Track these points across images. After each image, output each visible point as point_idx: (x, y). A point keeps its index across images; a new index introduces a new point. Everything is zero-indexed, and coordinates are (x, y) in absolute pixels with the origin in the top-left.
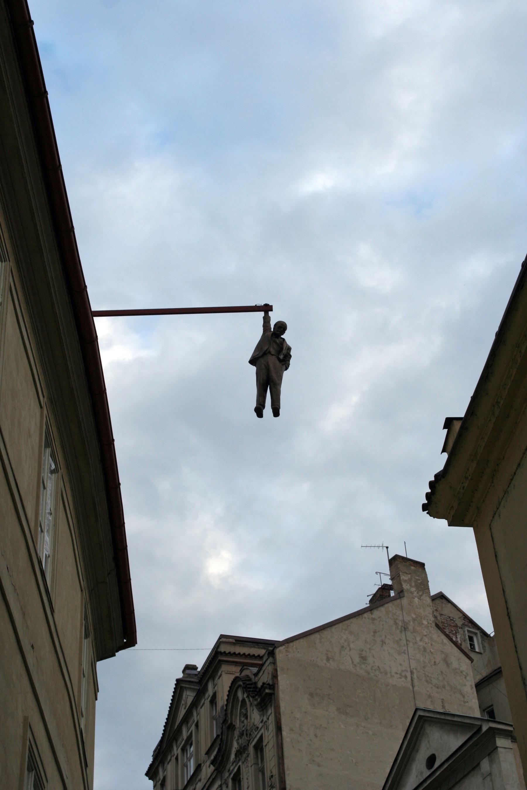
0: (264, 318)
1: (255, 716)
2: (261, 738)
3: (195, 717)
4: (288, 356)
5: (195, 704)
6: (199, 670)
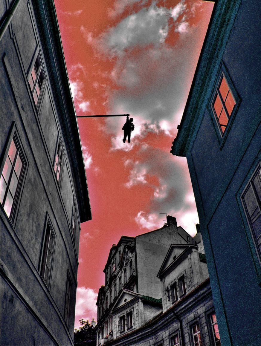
0: (127, 118)
1: (130, 255)
2: (131, 260)
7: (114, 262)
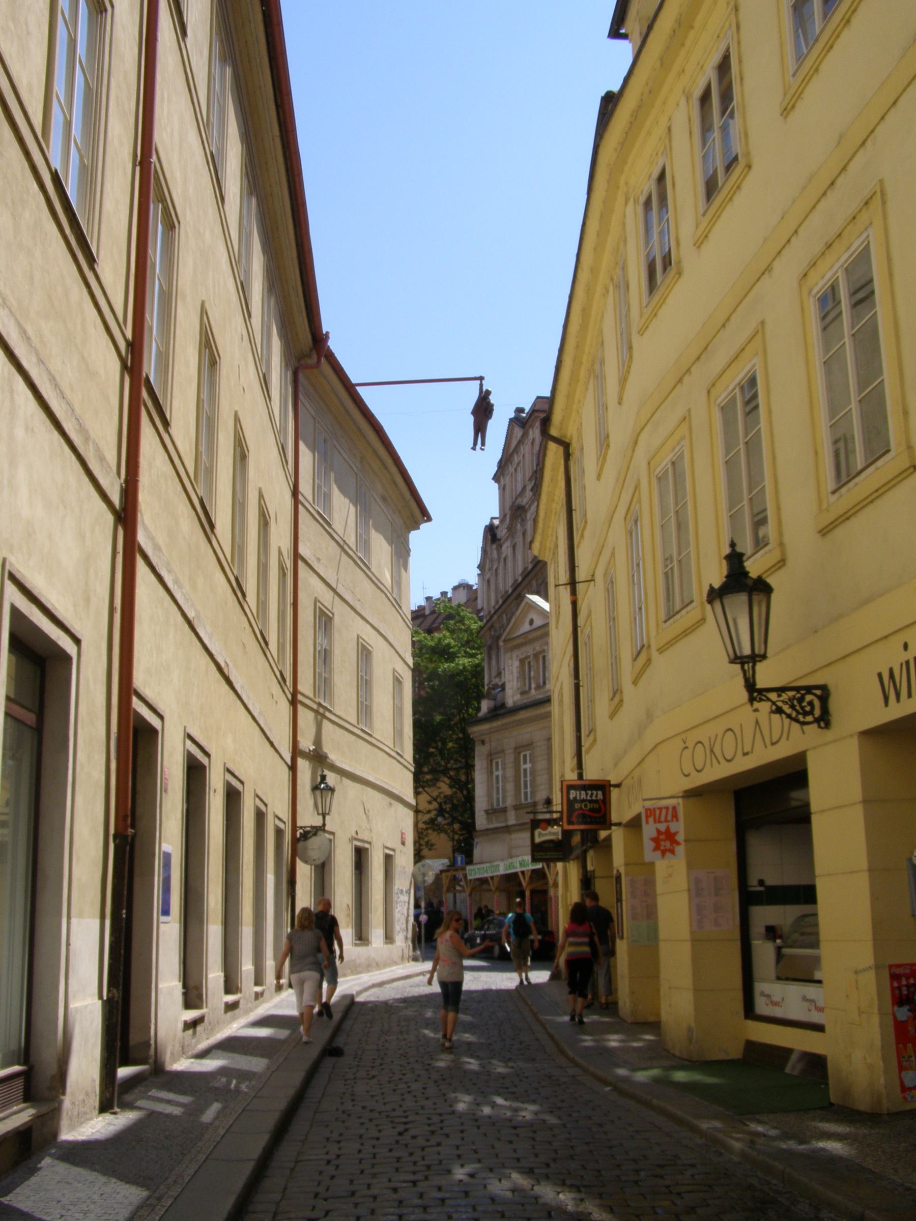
6: (526, 411)
7: (519, 463)
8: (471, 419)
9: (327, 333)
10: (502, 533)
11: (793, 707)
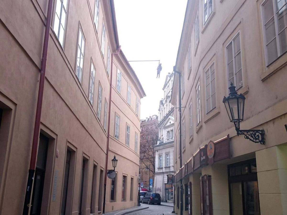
3: (169, 83)
4: (161, 69)
5: (169, 80)
7: (169, 86)
8: (156, 71)
9: (120, 46)
10: (164, 102)
11: (252, 137)
